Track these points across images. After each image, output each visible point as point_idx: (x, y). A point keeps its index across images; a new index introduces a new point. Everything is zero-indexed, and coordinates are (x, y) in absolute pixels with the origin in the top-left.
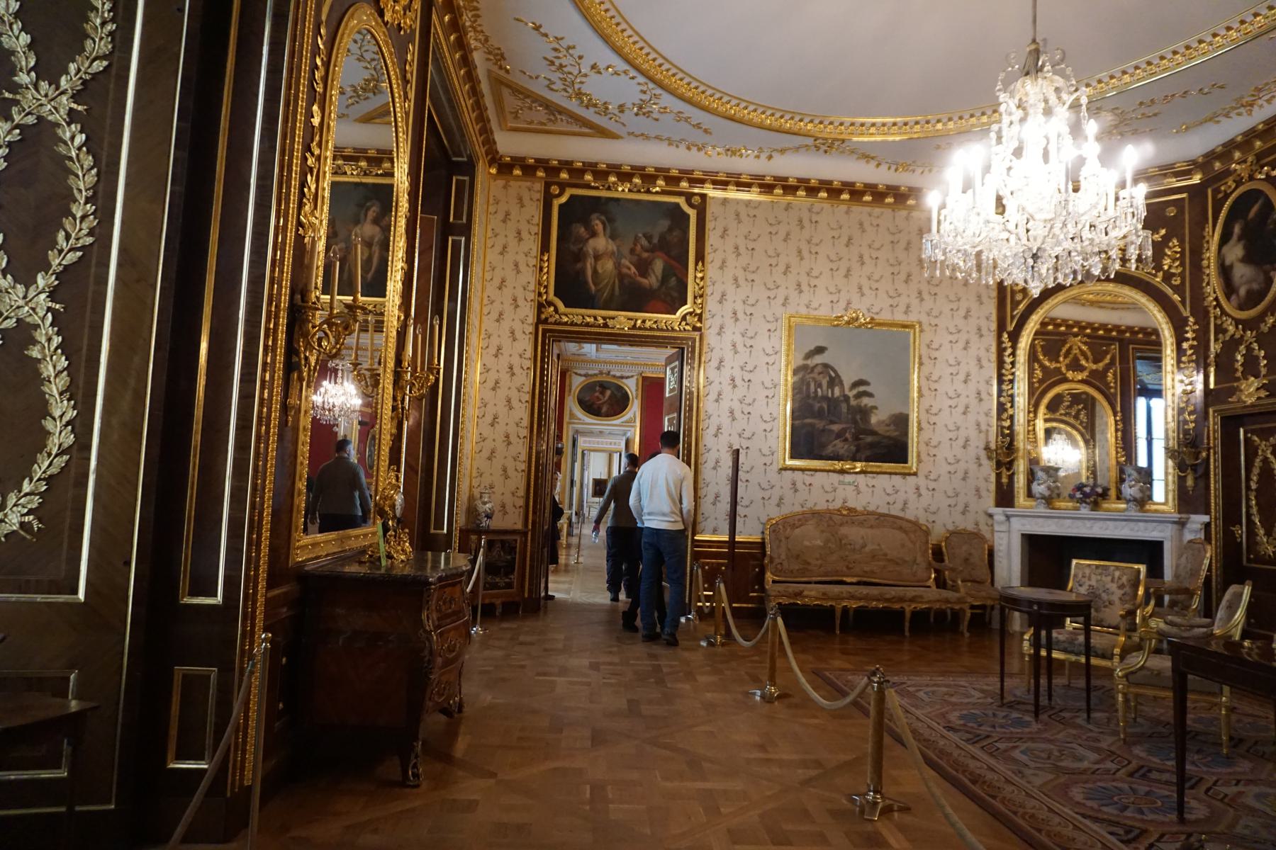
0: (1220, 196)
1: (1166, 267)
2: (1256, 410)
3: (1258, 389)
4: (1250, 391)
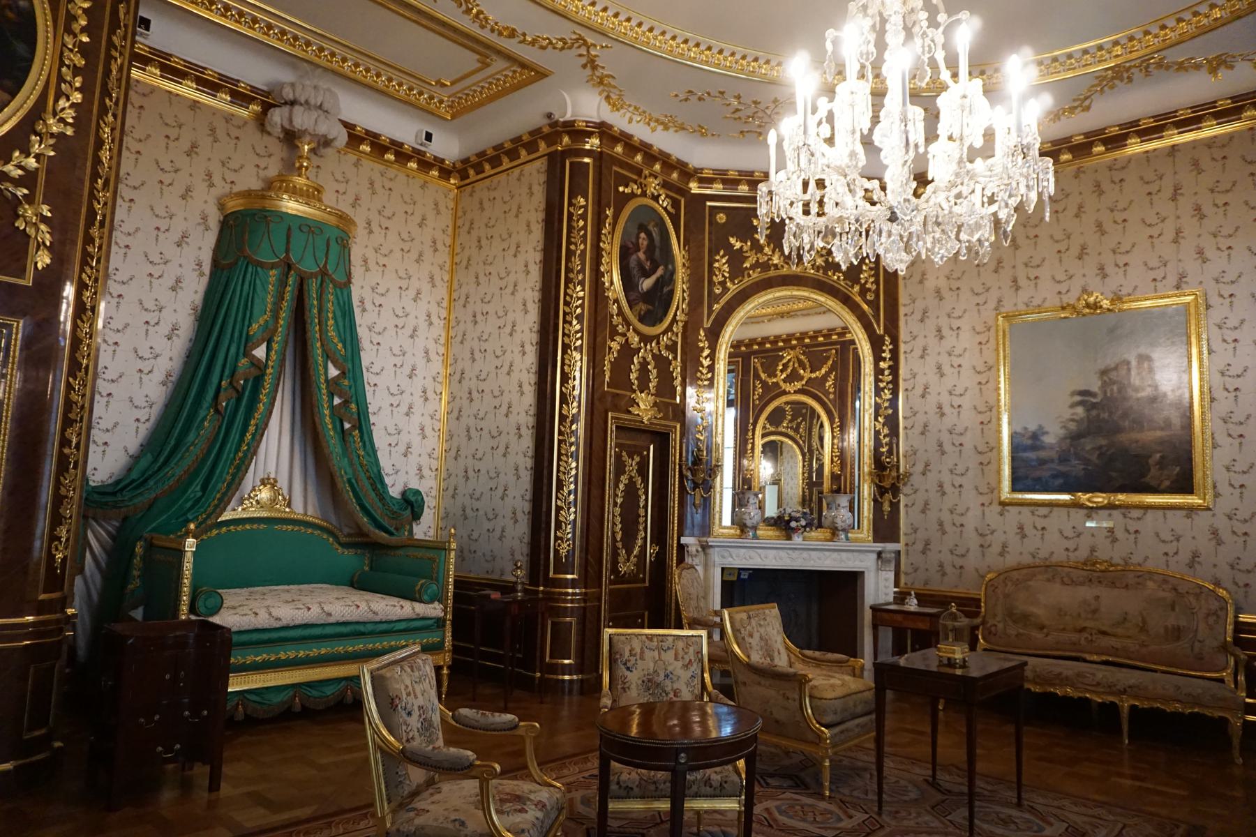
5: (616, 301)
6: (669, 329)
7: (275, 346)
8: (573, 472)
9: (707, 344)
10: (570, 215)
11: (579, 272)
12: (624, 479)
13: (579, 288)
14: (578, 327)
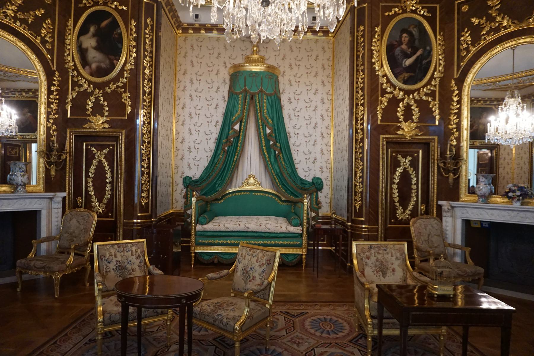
0: (81, 5)
1: (43, 35)
2: (101, 134)
3: (103, 123)
4: (99, 123)
5: (385, 75)
6: (429, 83)
7: (243, 124)
8: (361, 167)
9: (456, 88)
10: (357, 36)
11: (361, 65)
12: (400, 170)
13: (361, 74)
14: (362, 93)
